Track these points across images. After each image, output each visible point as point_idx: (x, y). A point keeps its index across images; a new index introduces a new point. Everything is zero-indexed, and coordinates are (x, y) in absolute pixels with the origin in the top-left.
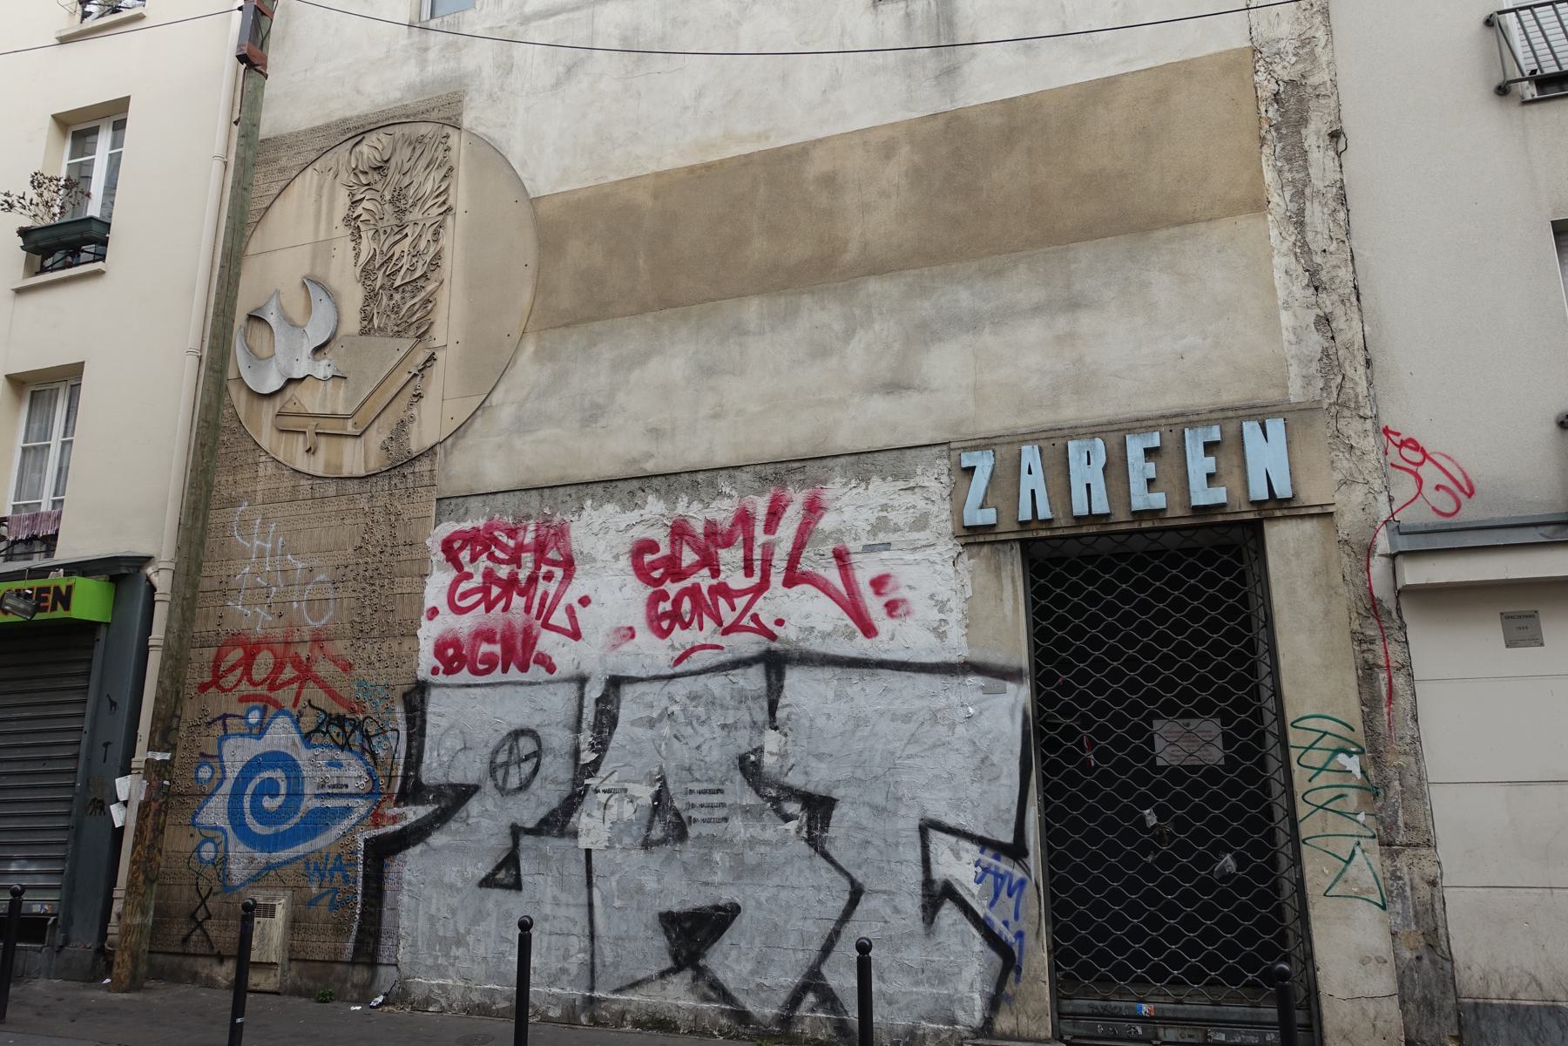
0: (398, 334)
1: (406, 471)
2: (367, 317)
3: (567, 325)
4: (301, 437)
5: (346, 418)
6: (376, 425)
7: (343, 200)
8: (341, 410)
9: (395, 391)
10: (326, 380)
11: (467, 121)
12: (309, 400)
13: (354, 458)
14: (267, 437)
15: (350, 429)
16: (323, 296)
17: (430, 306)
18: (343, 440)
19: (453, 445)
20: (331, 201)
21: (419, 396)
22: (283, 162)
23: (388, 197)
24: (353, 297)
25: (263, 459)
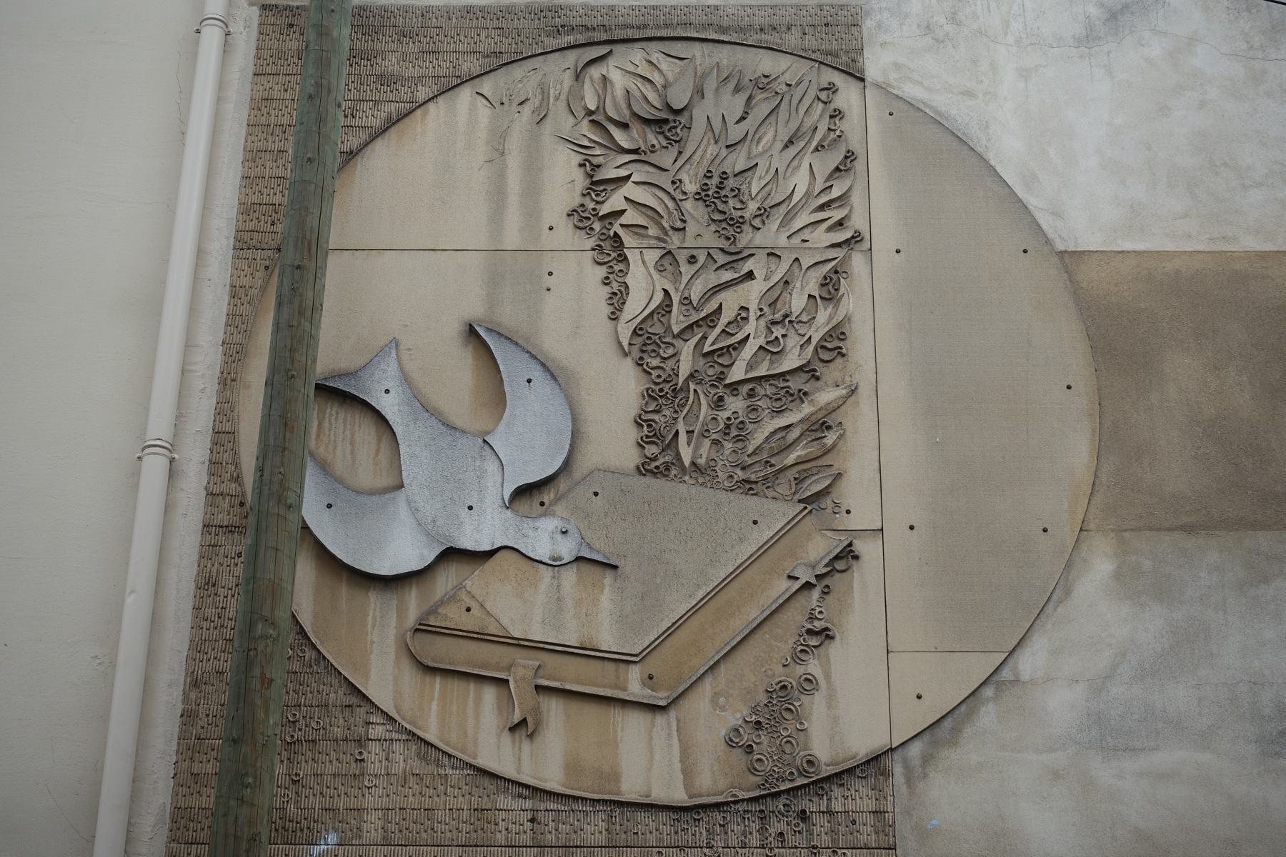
0: (748, 486)
1: (804, 803)
2: (653, 434)
3: (1189, 529)
4: (489, 694)
5: (622, 660)
6: (707, 687)
7: (563, 180)
8: (607, 640)
9: (754, 613)
10: (555, 564)
11: (875, 65)
12: (513, 605)
13: (649, 760)
14: (385, 678)
15: (634, 686)
16: (537, 374)
17: (830, 438)
18: (616, 714)
19: (927, 759)
20: (533, 168)
21: (826, 635)
22: (391, 64)
23: (691, 187)
24: (615, 392)
25: (378, 731)
